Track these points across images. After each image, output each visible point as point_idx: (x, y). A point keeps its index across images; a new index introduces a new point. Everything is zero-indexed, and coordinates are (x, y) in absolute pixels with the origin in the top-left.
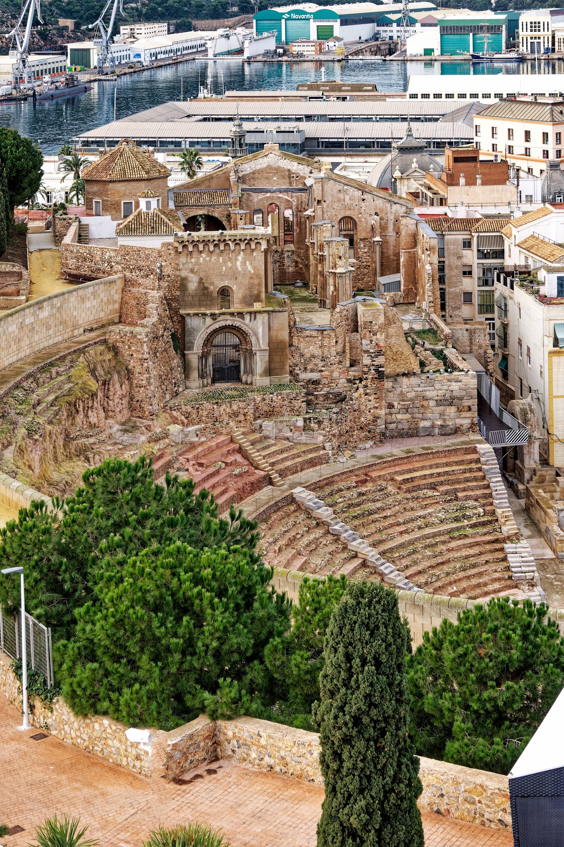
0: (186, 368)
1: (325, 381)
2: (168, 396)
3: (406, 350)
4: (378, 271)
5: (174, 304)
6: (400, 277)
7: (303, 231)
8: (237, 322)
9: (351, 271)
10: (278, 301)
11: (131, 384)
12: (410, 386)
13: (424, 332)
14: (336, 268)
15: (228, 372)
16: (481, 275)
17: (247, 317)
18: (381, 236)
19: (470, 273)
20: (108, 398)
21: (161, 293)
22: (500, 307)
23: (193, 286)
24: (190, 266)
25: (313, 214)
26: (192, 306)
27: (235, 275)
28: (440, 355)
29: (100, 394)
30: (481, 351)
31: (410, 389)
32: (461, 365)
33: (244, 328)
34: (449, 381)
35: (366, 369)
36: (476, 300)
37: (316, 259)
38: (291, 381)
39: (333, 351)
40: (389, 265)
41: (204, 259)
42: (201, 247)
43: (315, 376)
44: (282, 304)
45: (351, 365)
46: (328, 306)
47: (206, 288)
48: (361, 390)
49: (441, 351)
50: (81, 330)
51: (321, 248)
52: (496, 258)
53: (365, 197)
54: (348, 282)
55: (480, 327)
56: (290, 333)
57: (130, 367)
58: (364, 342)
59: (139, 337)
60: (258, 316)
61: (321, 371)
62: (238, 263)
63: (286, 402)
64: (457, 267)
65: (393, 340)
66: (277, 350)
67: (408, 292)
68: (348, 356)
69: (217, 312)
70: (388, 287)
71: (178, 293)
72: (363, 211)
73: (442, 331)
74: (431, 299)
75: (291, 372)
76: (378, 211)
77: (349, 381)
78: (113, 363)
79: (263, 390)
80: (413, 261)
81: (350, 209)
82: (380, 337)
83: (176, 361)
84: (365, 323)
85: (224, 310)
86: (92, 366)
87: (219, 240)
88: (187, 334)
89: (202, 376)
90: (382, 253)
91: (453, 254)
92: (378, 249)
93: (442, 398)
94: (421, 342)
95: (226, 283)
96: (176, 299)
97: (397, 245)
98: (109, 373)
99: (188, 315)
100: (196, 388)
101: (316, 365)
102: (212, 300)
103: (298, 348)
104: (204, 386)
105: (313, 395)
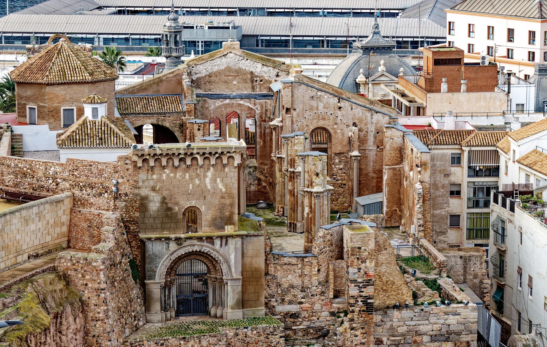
0: (146, 299)
1: (304, 314)
2: (127, 331)
3: (398, 279)
4: (355, 190)
5: (131, 228)
6: (382, 197)
7: (268, 144)
8: (206, 248)
9: (329, 190)
10: (252, 224)
11: (86, 318)
12: (403, 320)
13: (414, 259)
14: (312, 187)
15: (194, 305)
16: (472, 195)
17: (218, 242)
18: (359, 150)
19: (458, 193)
20: (60, 332)
21: (117, 214)
22: (496, 232)
23: (154, 206)
24: (152, 183)
25: (280, 124)
26: (153, 229)
27: (203, 194)
28: (433, 285)
29: (52, 330)
30: (477, 281)
31: (402, 323)
32: (459, 296)
33: (214, 254)
34: (446, 313)
35: (352, 301)
36: (464, 223)
37: (283, 176)
38: (266, 315)
39: (315, 280)
40: (369, 183)
41: (168, 175)
42: (164, 161)
43: (293, 308)
44: (258, 227)
45: (336, 297)
46: (299, 231)
47: (170, 209)
48: (346, 325)
49: (435, 281)
50: (26, 256)
51: (292, 163)
52: (489, 176)
53: (342, 104)
54: (326, 202)
55: (475, 254)
56: (266, 260)
57: (84, 298)
58: (351, 270)
59: (94, 264)
60: (230, 241)
61: (301, 303)
62: (208, 180)
63: (262, 338)
64: (443, 186)
65: (383, 269)
66: (251, 278)
67: (391, 215)
68: (332, 286)
69: (183, 236)
70: (369, 209)
71: (137, 214)
72: (338, 121)
73: (435, 259)
74: (421, 222)
75: (266, 304)
76: (356, 121)
77: (333, 314)
78: (65, 294)
79: (234, 324)
80: (398, 178)
81: (324, 119)
82: (370, 265)
83: (135, 292)
84: (353, 249)
85: (190, 234)
86: (41, 297)
87: (186, 154)
88: (147, 261)
89: (165, 308)
90: (360, 170)
91: (440, 171)
92: (355, 165)
93: (438, 333)
94: (411, 271)
95: (193, 203)
96: (135, 222)
97: (380, 160)
98: (61, 305)
99: (150, 239)
100: (159, 322)
101: (295, 296)
102: (177, 222)
103: (274, 277)
104: (167, 320)
105: (290, 329)
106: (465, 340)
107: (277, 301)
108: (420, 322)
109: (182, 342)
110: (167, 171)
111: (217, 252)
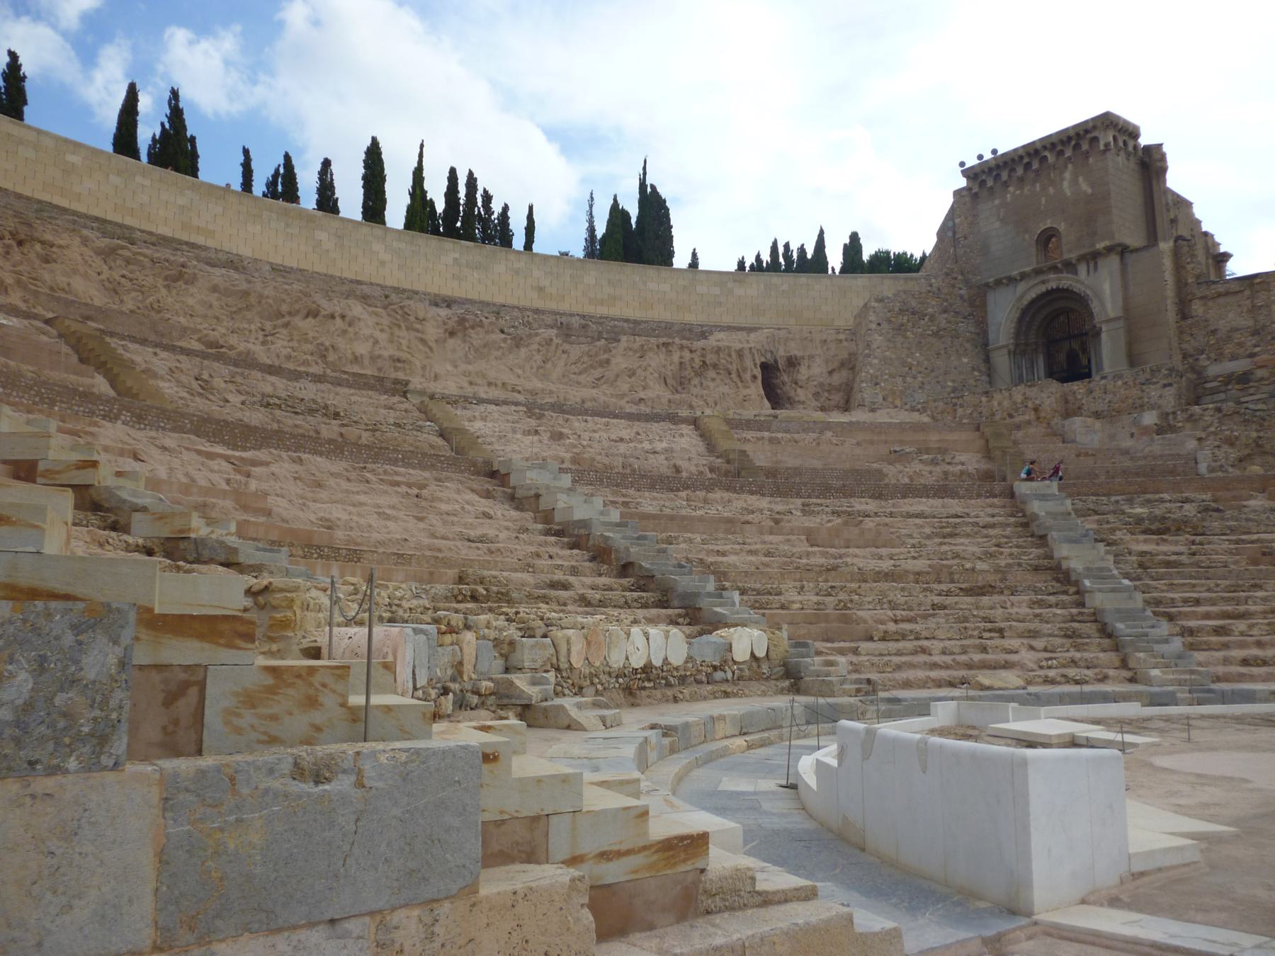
17: (1082, 269)
33: (1077, 287)
42: (1005, 176)
62: (1066, 184)
101: (1241, 345)
107: (1209, 358)
109: (984, 399)
110: (1011, 189)
111: (1082, 283)
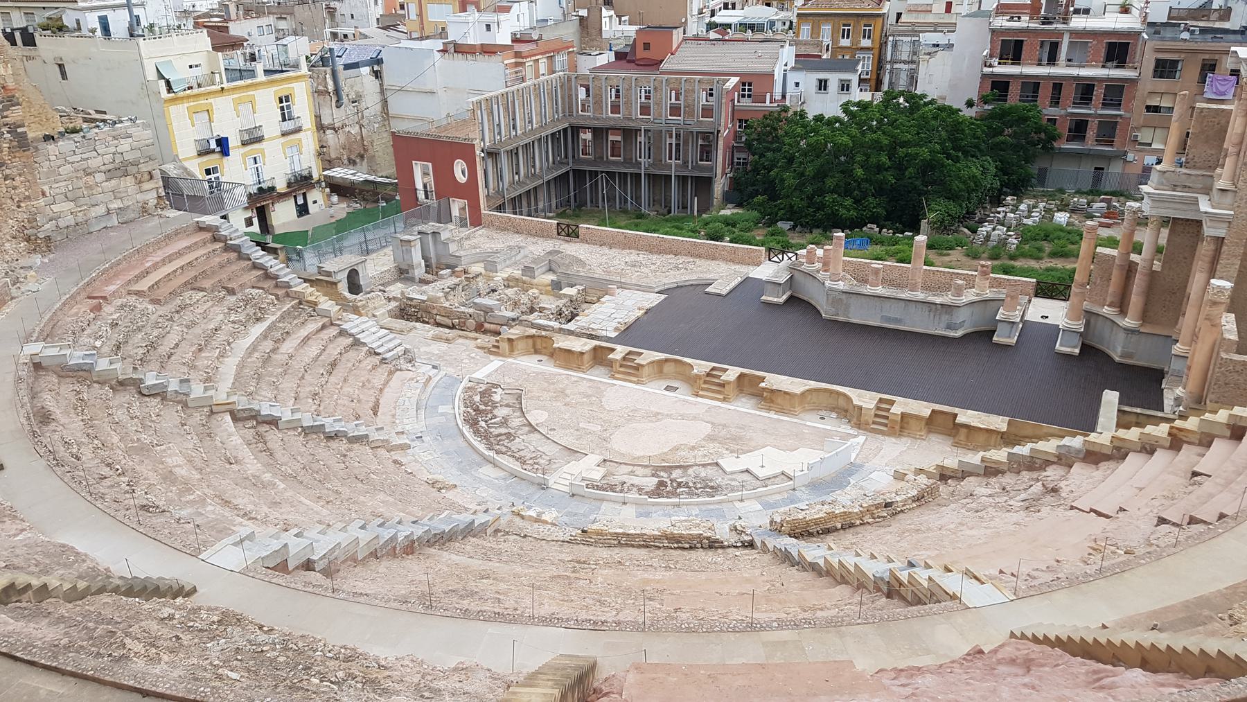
12: (63, 157)
31: (61, 162)
93: (111, 167)
106: (145, 170)
108: (84, 156)
